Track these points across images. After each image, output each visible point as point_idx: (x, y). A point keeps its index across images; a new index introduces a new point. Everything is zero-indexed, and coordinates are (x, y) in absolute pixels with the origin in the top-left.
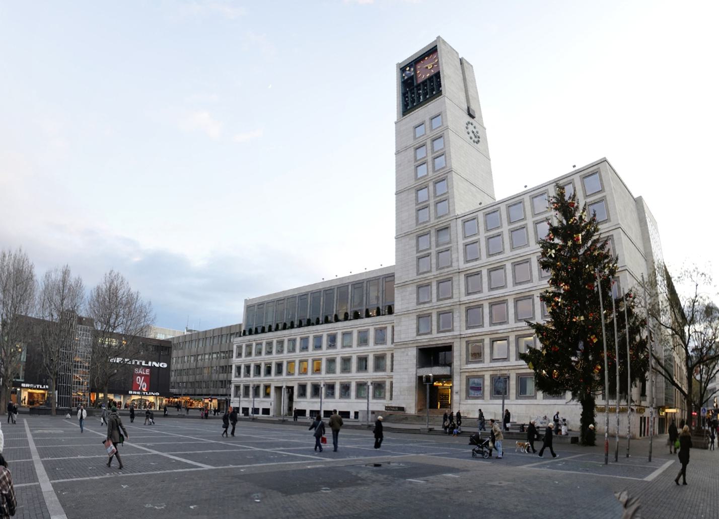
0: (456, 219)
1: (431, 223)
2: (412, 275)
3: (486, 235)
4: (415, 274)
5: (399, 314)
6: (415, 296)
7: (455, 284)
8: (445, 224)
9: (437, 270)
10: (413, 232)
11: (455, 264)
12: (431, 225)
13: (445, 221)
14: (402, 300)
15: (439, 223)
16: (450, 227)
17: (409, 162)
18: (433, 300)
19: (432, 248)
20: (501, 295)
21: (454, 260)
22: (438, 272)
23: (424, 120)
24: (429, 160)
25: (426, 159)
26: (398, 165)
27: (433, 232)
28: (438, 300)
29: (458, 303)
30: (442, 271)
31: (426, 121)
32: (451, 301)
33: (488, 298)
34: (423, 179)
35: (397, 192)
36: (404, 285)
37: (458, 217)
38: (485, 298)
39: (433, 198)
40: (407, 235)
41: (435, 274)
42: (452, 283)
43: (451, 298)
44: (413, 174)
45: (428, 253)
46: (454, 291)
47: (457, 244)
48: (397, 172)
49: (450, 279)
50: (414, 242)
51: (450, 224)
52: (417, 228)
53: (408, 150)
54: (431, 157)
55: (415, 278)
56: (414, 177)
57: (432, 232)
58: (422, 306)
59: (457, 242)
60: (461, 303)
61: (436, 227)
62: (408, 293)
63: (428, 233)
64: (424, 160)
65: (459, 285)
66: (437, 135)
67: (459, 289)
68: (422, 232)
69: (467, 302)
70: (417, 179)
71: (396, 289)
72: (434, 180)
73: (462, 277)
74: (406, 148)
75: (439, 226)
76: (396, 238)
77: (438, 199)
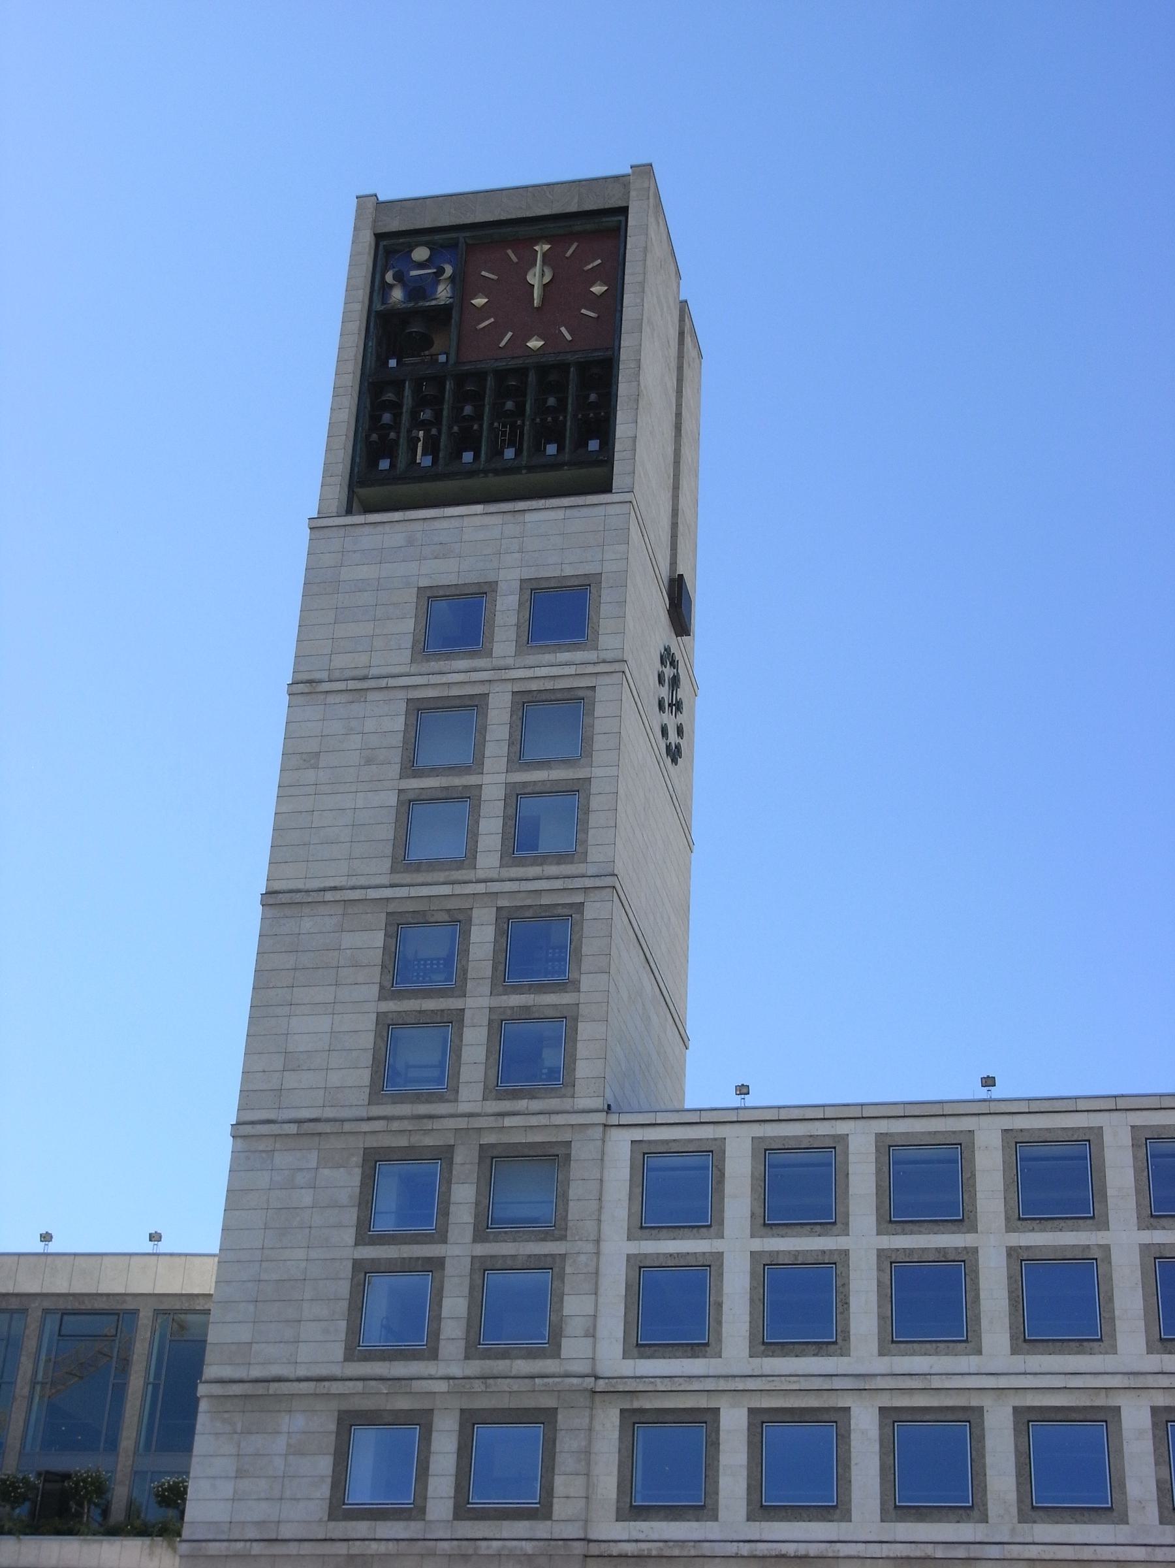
0: (605, 1125)
1: (463, 1108)
2: (320, 1348)
3: (758, 1245)
4: (338, 1351)
5: (213, 1549)
6: (325, 1465)
7: (567, 1444)
8: (539, 1138)
9: (467, 1358)
10: (347, 1127)
11: (573, 1347)
12: (462, 1123)
13: (543, 1120)
14: (240, 1474)
15: (508, 1122)
16: (569, 1155)
17: (369, 762)
18: (430, 1505)
19: (453, 1234)
20: (813, 1550)
21: (574, 1328)
22: (475, 1367)
23: (491, 578)
24: (486, 793)
25: (472, 780)
26: (300, 758)
27: (465, 1159)
28: (463, 1510)
29: (579, 1548)
30: (500, 1366)
31: (502, 587)
32: (541, 1529)
33: (745, 1549)
34: (441, 876)
35: (269, 893)
36: (262, 1396)
37: (614, 1119)
38: (732, 1549)
39: (486, 989)
40: (308, 1131)
41: (455, 1370)
42: (550, 1445)
43: (543, 1512)
44: (386, 832)
45: (428, 1260)
46: (559, 1481)
47: (598, 1253)
48: (285, 790)
49: (546, 1417)
50: (348, 1180)
51: (568, 1144)
52: (376, 1111)
53: (371, 696)
54: (502, 778)
55: (336, 1371)
56: (388, 850)
57: (458, 1159)
58: (361, 1528)
59: (598, 1241)
60: (594, 1549)
61: (490, 1139)
62: (280, 1444)
63: (445, 1154)
64: (457, 781)
65: (587, 1454)
66: (549, 685)
67: (587, 1475)
68: (403, 1142)
69: (629, 1548)
70: (403, 861)
71: (203, 1406)
72: (503, 902)
73: (609, 1421)
74: (361, 685)
75: (506, 1139)
76: (242, 1131)
77: (515, 1000)
